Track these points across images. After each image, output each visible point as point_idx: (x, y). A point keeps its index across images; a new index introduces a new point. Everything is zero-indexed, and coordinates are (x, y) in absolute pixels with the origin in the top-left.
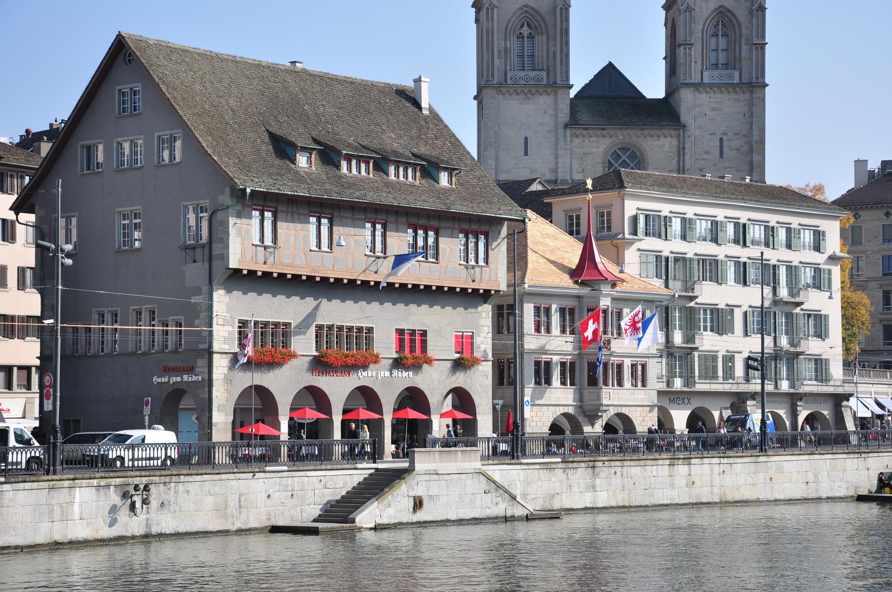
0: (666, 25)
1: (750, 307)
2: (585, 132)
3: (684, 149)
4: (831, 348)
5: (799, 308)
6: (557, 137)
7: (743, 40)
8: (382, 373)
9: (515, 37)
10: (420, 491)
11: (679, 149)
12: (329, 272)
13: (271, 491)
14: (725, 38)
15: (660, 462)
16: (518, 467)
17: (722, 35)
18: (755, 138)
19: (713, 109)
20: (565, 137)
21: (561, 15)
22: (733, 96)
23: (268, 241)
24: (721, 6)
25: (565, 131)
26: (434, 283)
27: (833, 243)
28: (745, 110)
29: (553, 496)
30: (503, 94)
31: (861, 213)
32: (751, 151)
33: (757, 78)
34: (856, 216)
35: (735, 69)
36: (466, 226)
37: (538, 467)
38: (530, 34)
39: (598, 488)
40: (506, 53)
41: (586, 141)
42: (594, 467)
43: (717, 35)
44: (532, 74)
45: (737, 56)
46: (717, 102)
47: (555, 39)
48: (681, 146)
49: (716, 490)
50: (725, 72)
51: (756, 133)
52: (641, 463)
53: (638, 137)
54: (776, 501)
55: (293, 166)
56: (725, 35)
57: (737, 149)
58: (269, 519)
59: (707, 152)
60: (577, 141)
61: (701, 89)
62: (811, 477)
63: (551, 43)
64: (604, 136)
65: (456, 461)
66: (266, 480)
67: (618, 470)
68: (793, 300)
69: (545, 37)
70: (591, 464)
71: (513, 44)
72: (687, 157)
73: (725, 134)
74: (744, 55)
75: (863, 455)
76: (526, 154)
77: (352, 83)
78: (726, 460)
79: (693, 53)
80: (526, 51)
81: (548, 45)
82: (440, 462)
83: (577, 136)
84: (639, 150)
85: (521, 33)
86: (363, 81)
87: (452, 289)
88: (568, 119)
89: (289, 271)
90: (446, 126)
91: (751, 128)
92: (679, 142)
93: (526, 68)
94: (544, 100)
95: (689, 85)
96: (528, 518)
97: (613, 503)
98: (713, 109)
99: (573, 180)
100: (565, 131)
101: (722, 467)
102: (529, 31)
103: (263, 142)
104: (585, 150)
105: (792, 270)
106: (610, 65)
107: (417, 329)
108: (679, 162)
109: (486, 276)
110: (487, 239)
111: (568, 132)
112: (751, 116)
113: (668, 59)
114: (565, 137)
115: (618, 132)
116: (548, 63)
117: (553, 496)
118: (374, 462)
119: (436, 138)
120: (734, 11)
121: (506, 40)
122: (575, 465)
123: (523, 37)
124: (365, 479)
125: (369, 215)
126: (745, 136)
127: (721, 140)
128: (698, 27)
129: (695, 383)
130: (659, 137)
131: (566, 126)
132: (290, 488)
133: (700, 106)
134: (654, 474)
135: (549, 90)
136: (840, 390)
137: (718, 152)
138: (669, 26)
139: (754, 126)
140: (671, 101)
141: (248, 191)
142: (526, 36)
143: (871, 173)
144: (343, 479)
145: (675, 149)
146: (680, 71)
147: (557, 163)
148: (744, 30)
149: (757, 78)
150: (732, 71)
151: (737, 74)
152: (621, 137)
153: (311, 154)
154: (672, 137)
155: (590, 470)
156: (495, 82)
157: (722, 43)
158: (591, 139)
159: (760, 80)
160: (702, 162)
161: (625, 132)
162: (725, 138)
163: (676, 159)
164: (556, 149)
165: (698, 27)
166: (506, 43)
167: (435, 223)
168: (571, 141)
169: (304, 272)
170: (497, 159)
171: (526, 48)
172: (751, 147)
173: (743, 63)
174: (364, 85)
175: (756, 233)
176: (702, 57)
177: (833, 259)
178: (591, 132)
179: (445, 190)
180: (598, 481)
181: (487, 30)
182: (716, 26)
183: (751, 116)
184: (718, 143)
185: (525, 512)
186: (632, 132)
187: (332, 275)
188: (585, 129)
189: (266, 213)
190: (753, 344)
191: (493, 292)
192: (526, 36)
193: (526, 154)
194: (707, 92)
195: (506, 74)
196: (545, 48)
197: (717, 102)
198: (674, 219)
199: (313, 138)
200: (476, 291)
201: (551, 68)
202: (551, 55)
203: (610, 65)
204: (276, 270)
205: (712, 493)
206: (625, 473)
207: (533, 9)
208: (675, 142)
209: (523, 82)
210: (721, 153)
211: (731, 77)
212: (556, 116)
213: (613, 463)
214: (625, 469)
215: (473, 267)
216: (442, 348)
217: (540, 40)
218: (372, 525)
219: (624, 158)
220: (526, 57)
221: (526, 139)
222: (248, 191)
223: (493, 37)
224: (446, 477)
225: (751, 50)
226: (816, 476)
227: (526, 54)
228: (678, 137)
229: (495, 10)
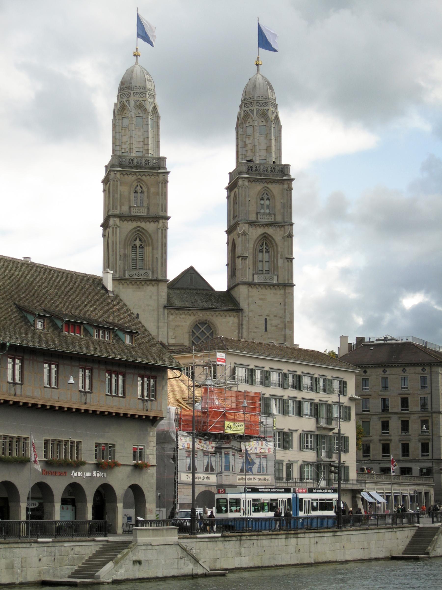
0: (228, 243)
1: (303, 431)
2: (177, 312)
3: (242, 325)
4: (350, 459)
5: (331, 432)
6: (159, 315)
7: (279, 256)
8: (87, 473)
9: (131, 247)
10: (140, 556)
11: (239, 324)
12: (56, 403)
13: (41, 556)
14: (267, 254)
15: (280, 536)
16: (195, 540)
17: (266, 252)
18: (288, 319)
20: (164, 314)
21: (162, 233)
22: (273, 291)
23: (17, 379)
24: (265, 233)
25: (164, 310)
26: (122, 411)
27: (351, 391)
28: (281, 300)
29: (215, 560)
30: (123, 285)
33: (288, 280)
34: (384, 371)
35: (274, 274)
36: (142, 372)
37: (207, 540)
38: (141, 245)
39: (243, 555)
40: (124, 257)
41: (178, 317)
42: (241, 540)
43: (262, 252)
44: (142, 272)
45: (276, 265)
46: (263, 295)
47: (157, 249)
48: (240, 323)
49: (312, 555)
50: (268, 276)
51: (288, 316)
52: (269, 537)
53: (212, 316)
54: (347, 562)
55: (33, 328)
56: (267, 252)
57: (276, 326)
58: (40, 576)
59: (256, 328)
60: (171, 317)
62: (366, 545)
63: (155, 252)
64: (190, 315)
65: (163, 536)
66: (38, 549)
67: (255, 542)
68: (328, 426)
69: (151, 248)
70: (239, 538)
71: (129, 251)
72: (244, 330)
73: (268, 316)
74: (280, 265)
75: (395, 530)
77: (63, 273)
78: (318, 535)
79: (247, 262)
80: (138, 256)
81: (153, 253)
82: (153, 537)
83: (172, 314)
84: (213, 325)
85: (135, 245)
86: (69, 271)
87: (133, 416)
88: (166, 302)
89: (30, 401)
90: (124, 304)
91: (285, 312)
92: (239, 321)
93: (138, 268)
94: (151, 289)
95: (244, 283)
96: (205, 576)
97: (252, 565)
98: (261, 299)
99: (168, 343)
100: (164, 310)
101: (316, 539)
102: (140, 243)
103: (12, 311)
104: (177, 324)
105: (329, 407)
106: (192, 268)
107: (109, 443)
108: (239, 333)
109: (154, 408)
110: (155, 382)
111: (166, 311)
112: (285, 305)
114: (164, 314)
115: (199, 313)
116: (152, 265)
117: (215, 560)
118: (105, 536)
119: (119, 311)
120: (274, 237)
121: (124, 249)
122: (229, 539)
123: (136, 247)
124: (100, 548)
125: (82, 363)
126: (281, 317)
127: (266, 319)
129: (333, 483)
130: (226, 316)
131: (165, 307)
132: (53, 554)
134: (277, 544)
135: (153, 283)
136: (355, 487)
137: (264, 328)
138: (231, 244)
139: (287, 311)
140: (233, 293)
141: (8, 344)
142: (138, 247)
143: (350, 344)
144: (83, 549)
146: (238, 273)
147: (158, 332)
148: (279, 249)
149: (288, 280)
151: (275, 277)
153: (44, 320)
154: (234, 317)
155: (238, 542)
157: (266, 257)
158: (181, 316)
159: (290, 282)
160: (253, 334)
161: (204, 313)
162: (268, 318)
163: (237, 331)
164: (158, 322)
166: (125, 251)
167: (123, 370)
168: (168, 317)
169: (40, 402)
171: (138, 255)
172: (285, 325)
173: (279, 270)
174: (71, 274)
175: (306, 381)
176: (253, 264)
177: (351, 399)
179: (131, 348)
180: (243, 549)
181: (113, 242)
182: (261, 246)
183: (285, 305)
184: (264, 322)
185: (204, 572)
187: (58, 404)
189: (16, 360)
190: (310, 456)
191: (158, 418)
192: (138, 247)
194: (257, 288)
195: (124, 271)
196: (151, 255)
198: (257, 371)
199: (43, 309)
200: (148, 417)
201: (155, 268)
202: (155, 260)
203: (192, 268)
204: (22, 400)
205: (310, 557)
206: (259, 544)
207: (143, 229)
208: (236, 320)
209: (135, 277)
211: (271, 279)
212: (158, 300)
213: (252, 538)
214: (259, 541)
215: (147, 401)
216: (124, 456)
217: (148, 250)
218: (110, 581)
219: (202, 329)
220: (138, 260)
222: (8, 344)
223: (116, 247)
224: (157, 547)
225: (284, 262)
226: (369, 544)
227: (138, 258)
228: (238, 317)
229: (118, 229)
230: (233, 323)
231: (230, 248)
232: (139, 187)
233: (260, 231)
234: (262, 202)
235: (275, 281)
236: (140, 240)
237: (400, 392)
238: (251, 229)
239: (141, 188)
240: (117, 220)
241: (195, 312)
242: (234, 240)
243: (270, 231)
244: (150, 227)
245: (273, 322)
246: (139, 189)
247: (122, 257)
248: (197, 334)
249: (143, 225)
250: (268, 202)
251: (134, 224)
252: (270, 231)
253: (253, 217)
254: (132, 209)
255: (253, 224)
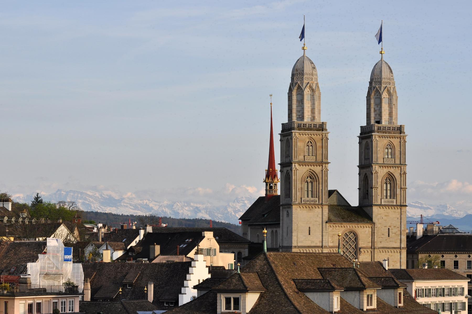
2: (334, 225)
19: (386, 216)
22: (393, 210)
28: (399, 216)
31: (431, 255)
32: (401, 235)
43: (386, 184)
44: (312, 199)
46: (387, 213)
57: (395, 233)
59: (383, 234)
60: (330, 229)
61: (381, 207)
76: (309, 234)
94: (318, 211)
98: (386, 216)
111: (328, 225)
112: (401, 219)
113: (362, 190)
123: (308, 183)
127: (389, 229)
128: (379, 180)
131: (326, 222)
133: (380, 214)
135: (320, 206)
138: (363, 176)
145: (371, 233)
148: (398, 182)
150: (393, 200)
151: (395, 201)
152: (349, 227)
156: (297, 203)
159: (404, 204)
161: (351, 225)
162: (390, 228)
165: (379, 180)
170: (297, 237)
178: (337, 225)
183: (401, 219)
184: (387, 230)
186: (354, 226)
188: (334, 224)
193: (309, 234)
195: (301, 198)
197: (387, 213)
201: (320, 197)
208: (370, 230)
210: (389, 234)
211: (393, 202)
221: (309, 228)
230: (369, 232)
231: (362, 178)
232: (310, 143)
233: (385, 170)
234: (386, 150)
235: (395, 204)
236: (310, 177)
237: (466, 271)
238: (380, 169)
239: (311, 143)
240: (297, 165)
241: (345, 225)
242: (366, 174)
243: (392, 170)
244: (318, 169)
245: (394, 231)
246: (310, 144)
247: (300, 190)
248: (346, 239)
249: (312, 168)
250: (390, 151)
251: (307, 168)
252: (392, 170)
253: (381, 161)
254: (306, 157)
255: (382, 166)
